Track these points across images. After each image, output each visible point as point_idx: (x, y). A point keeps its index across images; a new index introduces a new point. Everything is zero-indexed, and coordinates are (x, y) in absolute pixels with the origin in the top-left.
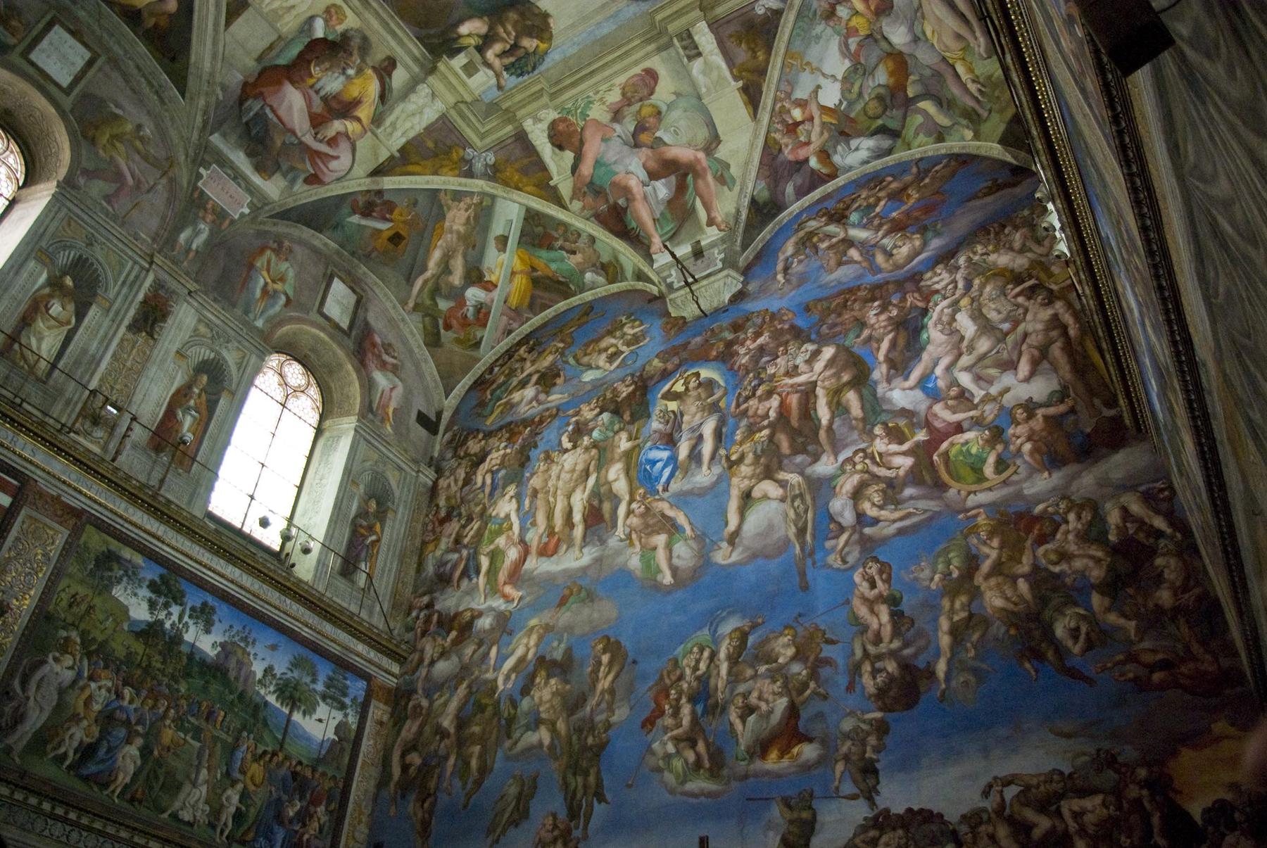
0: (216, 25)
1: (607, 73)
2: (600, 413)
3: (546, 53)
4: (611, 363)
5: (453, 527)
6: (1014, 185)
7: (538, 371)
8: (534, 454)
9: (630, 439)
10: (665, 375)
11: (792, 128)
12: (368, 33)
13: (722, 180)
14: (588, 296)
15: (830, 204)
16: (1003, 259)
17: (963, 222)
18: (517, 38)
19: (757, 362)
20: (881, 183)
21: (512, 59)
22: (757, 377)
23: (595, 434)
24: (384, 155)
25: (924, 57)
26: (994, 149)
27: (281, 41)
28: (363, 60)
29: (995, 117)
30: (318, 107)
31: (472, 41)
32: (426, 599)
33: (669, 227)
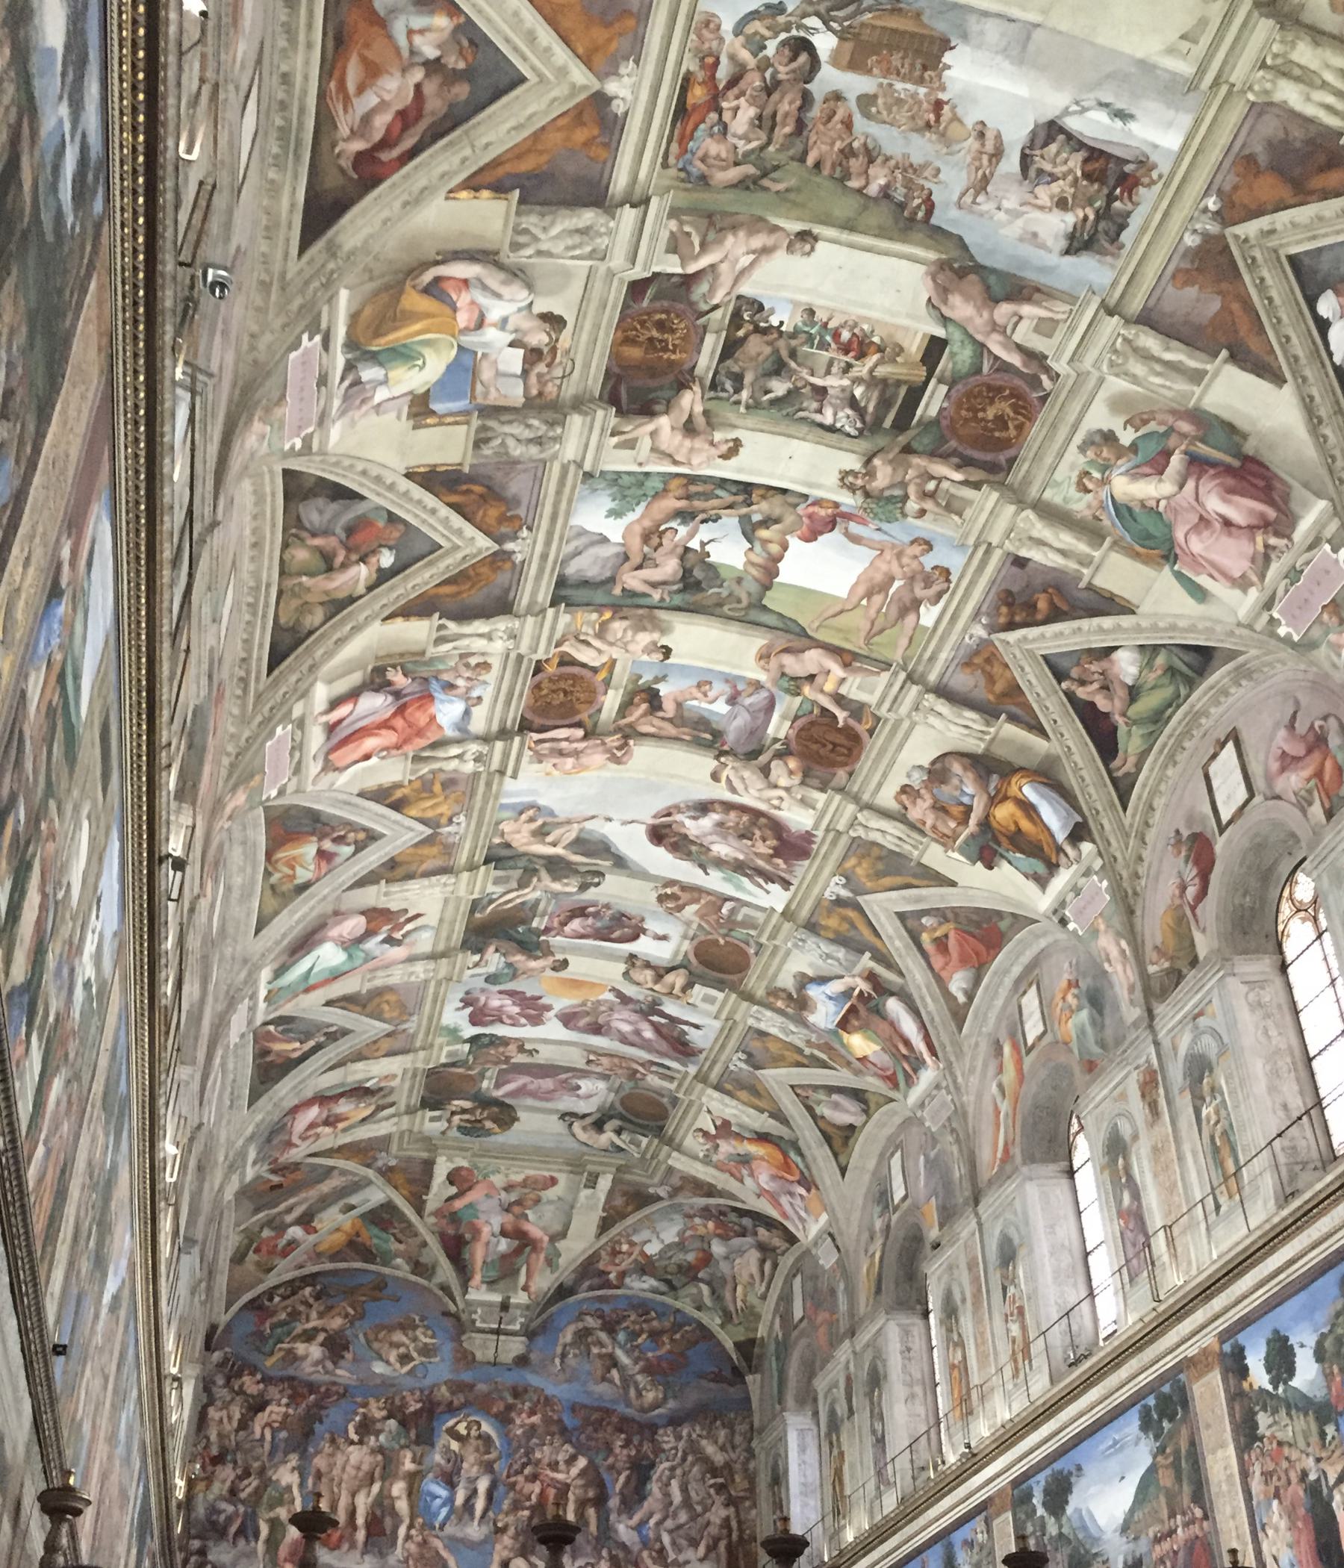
2: (388, 1418)
4: (402, 1364)
5: (227, 1473)
6: (731, 1385)
7: (324, 1330)
8: (317, 1426)
9: (414, 1461)
10: (452, 1410)
11: (615, 1253)
13: (550, 1263)
14: (386, 1270)
15: (607, 1308)
16: (710, 1449)
17: (692, 1397)
19: (529, 1440)
20: (647, 1313)
22: (527, 1454)
23: (382, 1438)
24: (329, 1146)
25: (724, 1267)
26: (729, 1345)
27: (342, 1085)
29: (741, 1329)
32: (196, 1544)
33: (493, 1274)
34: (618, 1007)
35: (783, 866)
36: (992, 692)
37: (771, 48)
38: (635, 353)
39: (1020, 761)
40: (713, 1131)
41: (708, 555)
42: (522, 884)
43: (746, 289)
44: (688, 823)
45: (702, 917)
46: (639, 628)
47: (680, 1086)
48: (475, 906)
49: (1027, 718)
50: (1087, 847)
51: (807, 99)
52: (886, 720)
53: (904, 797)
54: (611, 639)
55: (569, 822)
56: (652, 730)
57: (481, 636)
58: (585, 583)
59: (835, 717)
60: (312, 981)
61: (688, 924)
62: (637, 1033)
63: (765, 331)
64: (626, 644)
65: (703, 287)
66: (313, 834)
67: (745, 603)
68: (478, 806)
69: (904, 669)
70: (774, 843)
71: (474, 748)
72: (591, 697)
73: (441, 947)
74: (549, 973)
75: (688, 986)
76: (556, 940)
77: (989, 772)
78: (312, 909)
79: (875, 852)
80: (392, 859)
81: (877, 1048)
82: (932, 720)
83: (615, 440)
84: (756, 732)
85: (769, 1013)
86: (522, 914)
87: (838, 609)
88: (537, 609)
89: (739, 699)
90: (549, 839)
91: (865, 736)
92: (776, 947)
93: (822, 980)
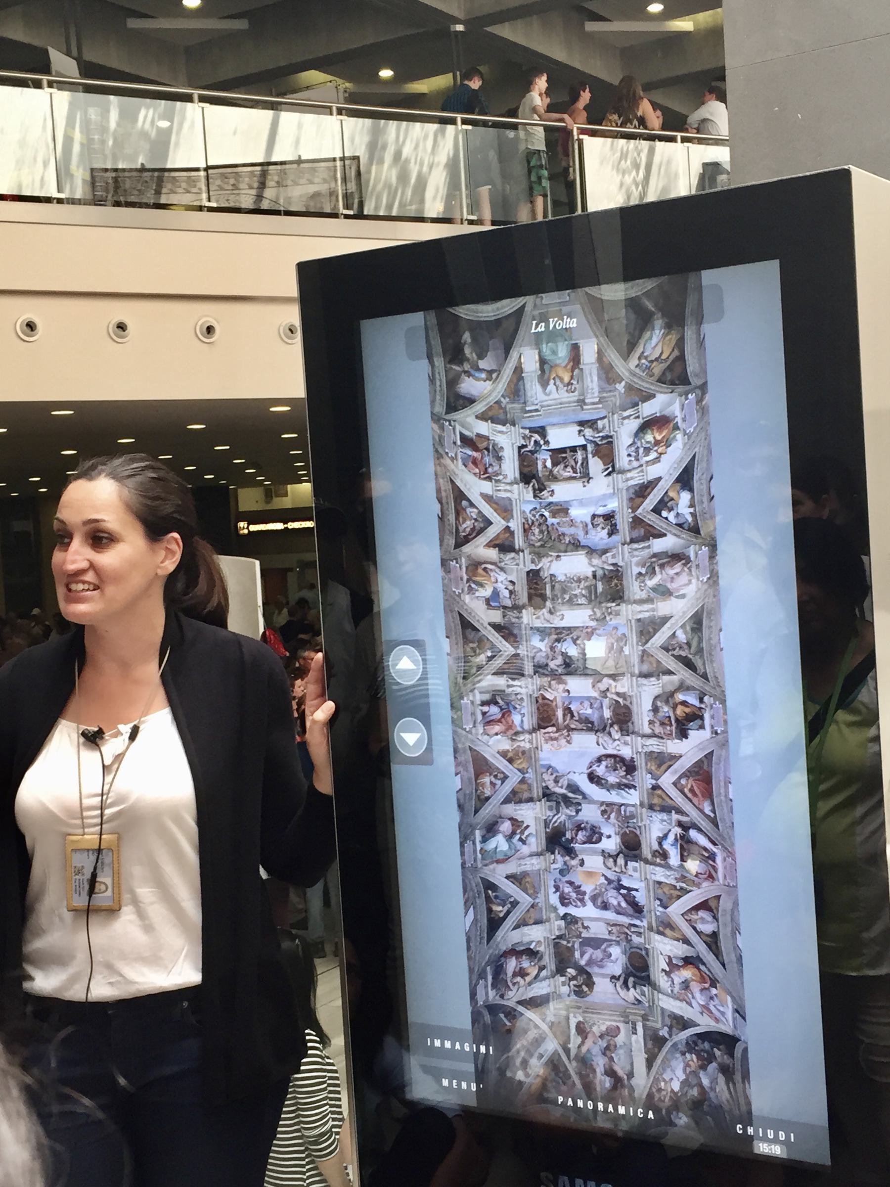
1: (604, 1017)
3: (588, 995)
18: (582, 984)
21: (577, 989)
31: (569, 976)
37: (537, 516)
38: (532, 591)
40: (668, 969)
42: (558, 812)
43: (551, 572)
46: (559, 683)
48: (546, 823)
51: (547, 525)
55: (563, 776)
58: (540, 667)
63: (559, 581)
65: (541, 573)
82: (645, 688)
83: (534, 616)
85: (658, 868)
90: (560, 785)
93: (665, 836)
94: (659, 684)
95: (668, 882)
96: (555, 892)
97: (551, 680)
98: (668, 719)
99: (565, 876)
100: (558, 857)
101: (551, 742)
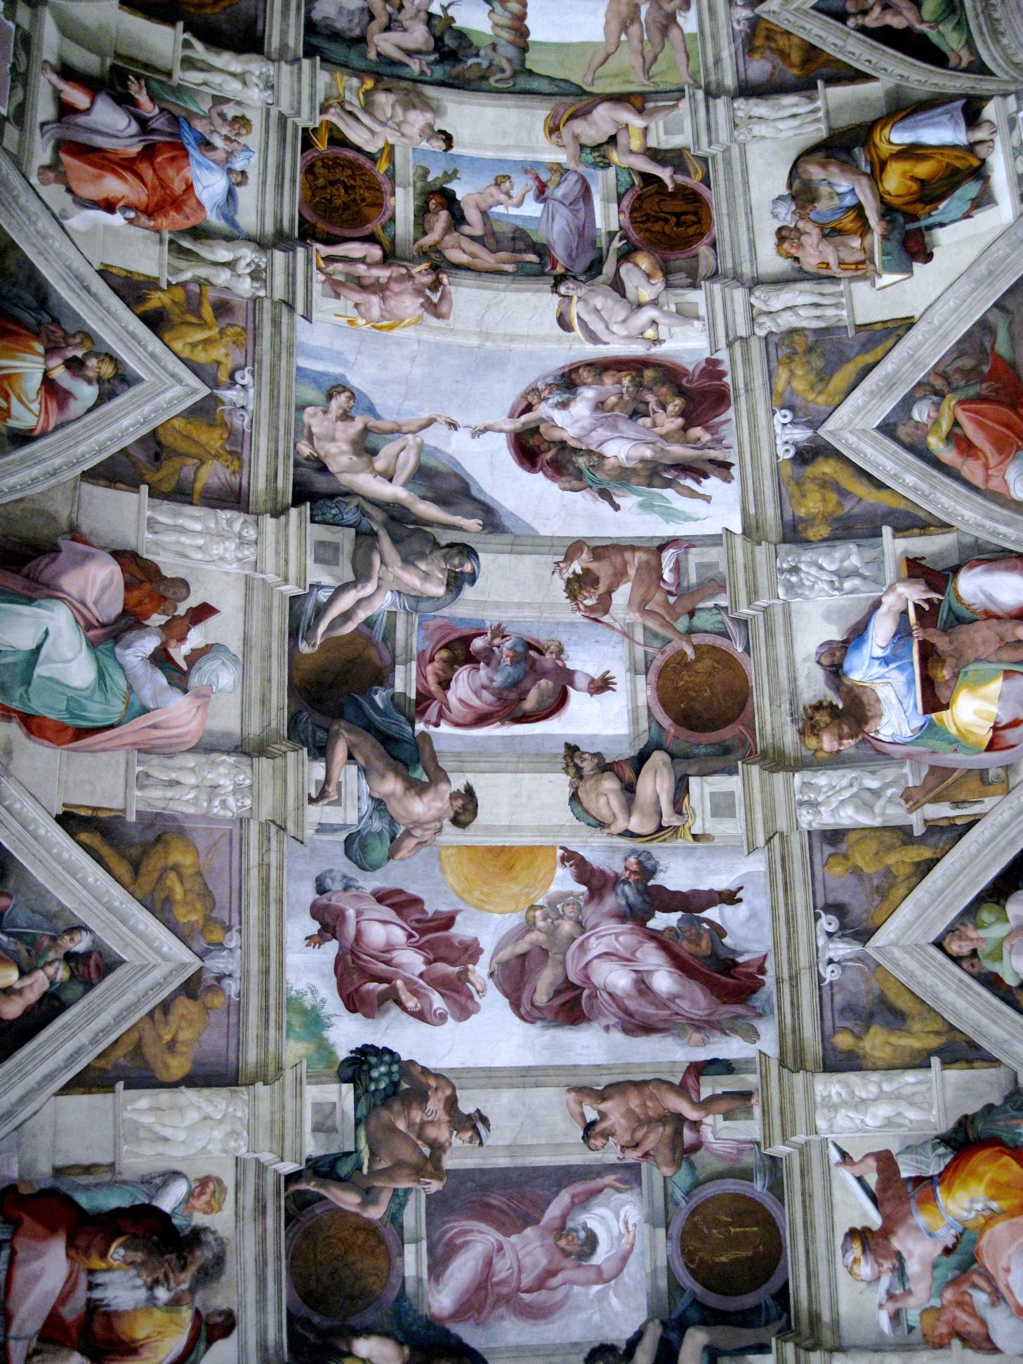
0: (50, 1077)
12: (230, 1257)
28: (192, 1290)
30: (73, 1310)
34: (591, 915)
35: (706, 437)
36: (792, 66)
39: (870, 116)
40: (874, 1219)
41: (453, 19)
42: (362, 574)
44: (559, 417)
45: (643, 611)
46: (408, 106)
47: (766, 1112)
49: (844, 72)
50: (990, 111)
52: (714, 157)
53: (786, 246)
54: (382, 118)
55: (397, 431)
56: (463, 258)
57: (234, 75)
58: (336, 36)
59: (658, 180)
60: (37, 705)
61: (627, 635)
62: (643, 986)
64: (399, 125)
66: (37, 336)
67: (508, 73)
68: (267, 359)
69: (699, 87)
70: (676, 404)
71: (247, 254)
72: (377, 197)
73: (255, 729)
74: (451, 835)
75: (681, 789)
76: (444, 734)
77: (848, 150)
78: (35, 480)
79: (800, 343)
80: (154, 432)
81: (997, 686)
82: (760, 129)
84: (584, 233)
85: (822, 779)
86: (372, 653)
87: (601, 56)
88: (290, 56)
89: (548, 193)
90: (380, 463)
91: (702, 189)
92: (765, 610)
93: (857, 634)
94: (812, 112)
95: (877, 822)
96: (315, 941)
97: (375, 89)
98: (852, 215)
99: (374, 868)
100: (348, 776)
101: (358, 297)
